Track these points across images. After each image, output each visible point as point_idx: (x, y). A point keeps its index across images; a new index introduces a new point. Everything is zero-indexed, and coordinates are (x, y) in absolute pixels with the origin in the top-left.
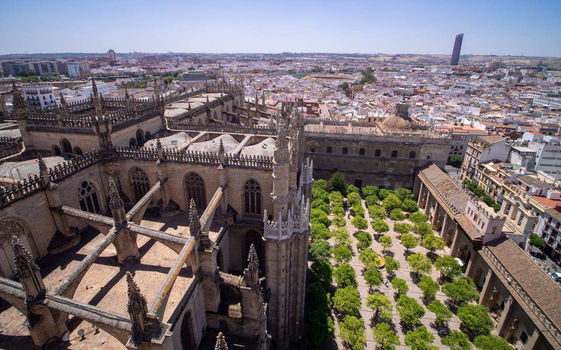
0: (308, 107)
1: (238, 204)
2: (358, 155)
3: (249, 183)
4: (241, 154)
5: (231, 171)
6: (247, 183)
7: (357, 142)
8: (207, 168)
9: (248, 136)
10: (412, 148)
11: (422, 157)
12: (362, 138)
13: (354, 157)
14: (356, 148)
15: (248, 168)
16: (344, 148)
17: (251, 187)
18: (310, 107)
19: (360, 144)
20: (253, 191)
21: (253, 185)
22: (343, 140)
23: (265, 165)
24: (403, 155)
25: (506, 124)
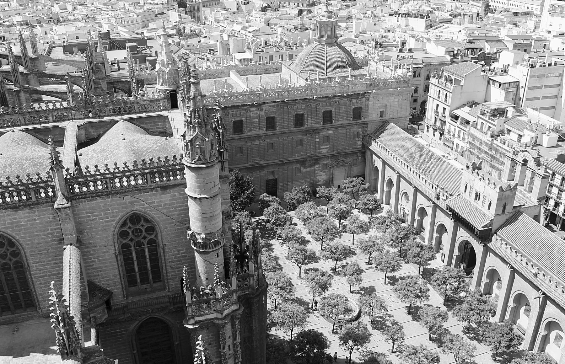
0: (132, 49)
1: (111, 275)
2: (263, 132)
3: (129, 224)
4: (83, 166)
5: (85, 206)
6: (124, 224)
7: (260, 105)
8: (22, 215)
9: (71, 128)
10: (354, 101)
11: (372, 115)
12: (269, 97)
13: (258, 137)
14: (258, 117)
15: (122, 192)
16: (235, 123)
17: (135, 232)
18: (132, 49)
19: (264, 108)
20: (140, 239)
21: (139, 227)
22: (232, 107)
23: (161, 177)
24: (342, 118)
25: (470, 42)
